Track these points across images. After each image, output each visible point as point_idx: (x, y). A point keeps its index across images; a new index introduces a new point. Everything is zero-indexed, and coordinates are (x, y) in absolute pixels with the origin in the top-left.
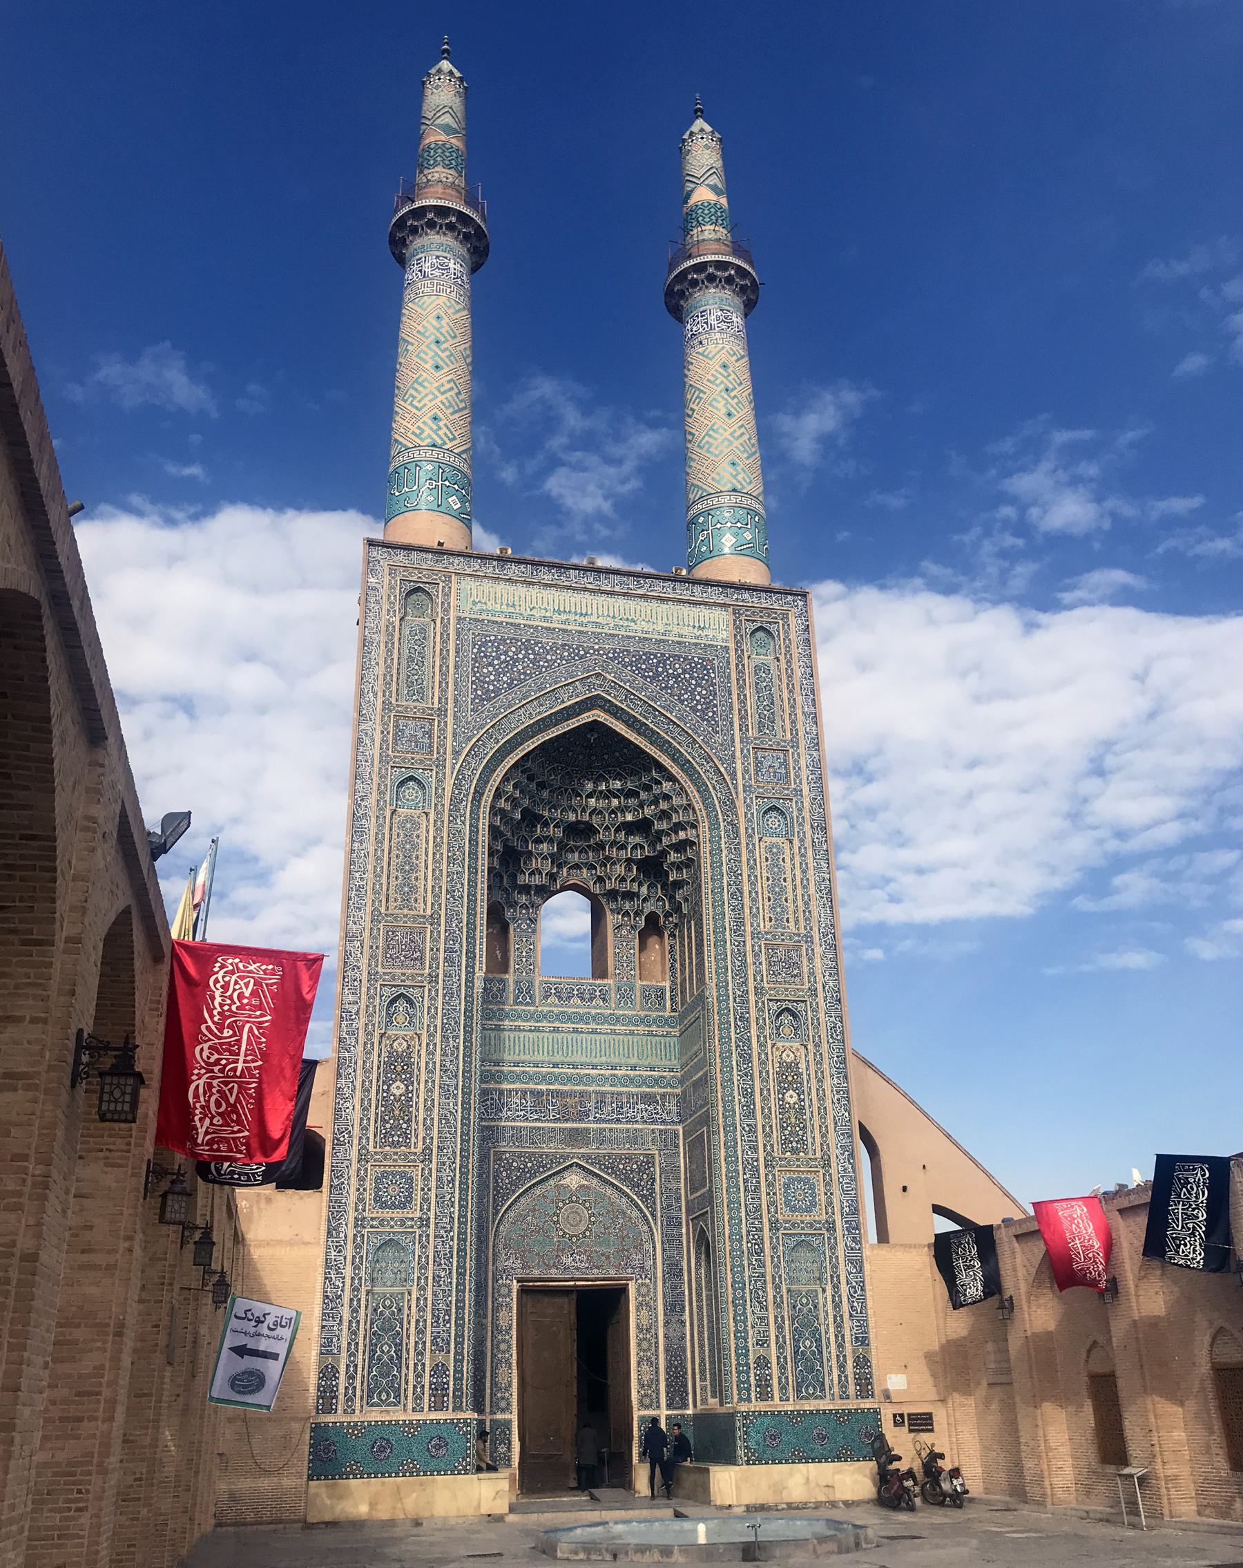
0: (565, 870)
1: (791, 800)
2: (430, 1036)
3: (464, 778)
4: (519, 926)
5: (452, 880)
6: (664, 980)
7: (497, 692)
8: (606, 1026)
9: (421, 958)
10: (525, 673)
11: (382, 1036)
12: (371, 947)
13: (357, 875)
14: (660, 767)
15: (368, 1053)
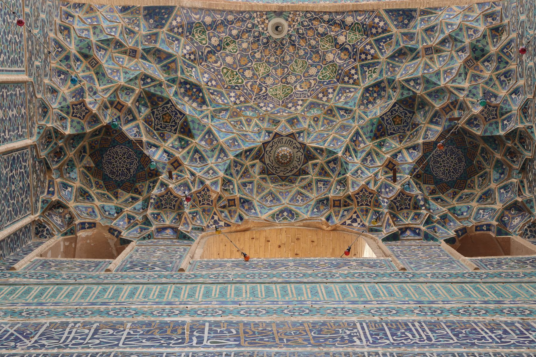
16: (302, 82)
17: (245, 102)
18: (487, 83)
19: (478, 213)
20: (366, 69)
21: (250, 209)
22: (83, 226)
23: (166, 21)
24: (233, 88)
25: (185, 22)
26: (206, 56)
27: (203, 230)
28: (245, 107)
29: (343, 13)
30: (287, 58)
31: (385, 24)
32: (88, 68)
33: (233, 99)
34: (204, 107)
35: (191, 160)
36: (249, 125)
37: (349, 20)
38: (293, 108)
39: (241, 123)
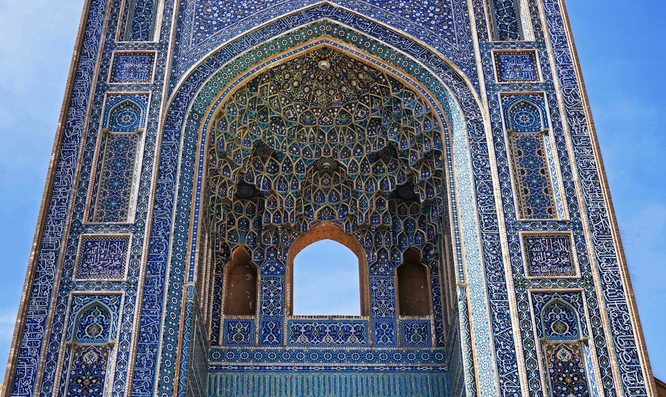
0: (316, 213)
1: (542, 95)
2: (122, 345)
3: (181, 100)
4: (267, 269)
5: (162, 191)
6: (429, 315)
7: (220, 25)
8: (363, 364)
9: (121, 268)
10: (249, 9)
11: (69, 347)
12: (67, 257)
13: (60, 190)
14: (397, 84)
15: (52, 364)
16: (338, 94)
17: (305, 109)
18: (428, 180)
19: (417, 234)
20: (373, 98)
21: (310, 209)
22: (233, 250)
23: (260, 80)
24: (298, 100)
25: (270, 75)
26: (283, 87)
27: (288, 248)
28: (305, 113)
29: (362, 63)
30: (329, 78)
31: (386, 81)
32: (225, 162)
33: (298, 110)
34: (283, 128)
35: (279, 183)
36: (308, 132)
37: (366, 68)
38: (332, 114)
39: (304, 132)
